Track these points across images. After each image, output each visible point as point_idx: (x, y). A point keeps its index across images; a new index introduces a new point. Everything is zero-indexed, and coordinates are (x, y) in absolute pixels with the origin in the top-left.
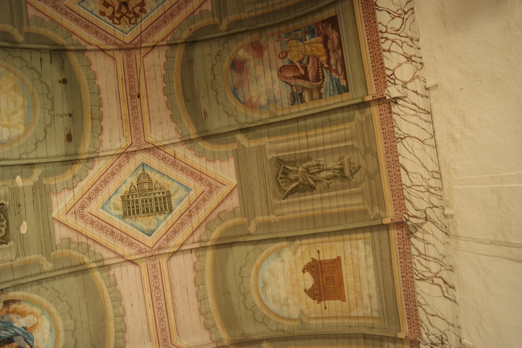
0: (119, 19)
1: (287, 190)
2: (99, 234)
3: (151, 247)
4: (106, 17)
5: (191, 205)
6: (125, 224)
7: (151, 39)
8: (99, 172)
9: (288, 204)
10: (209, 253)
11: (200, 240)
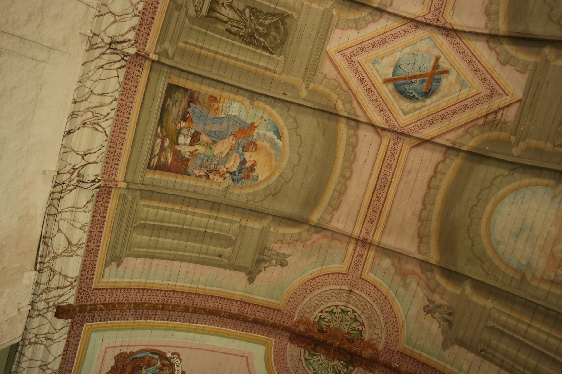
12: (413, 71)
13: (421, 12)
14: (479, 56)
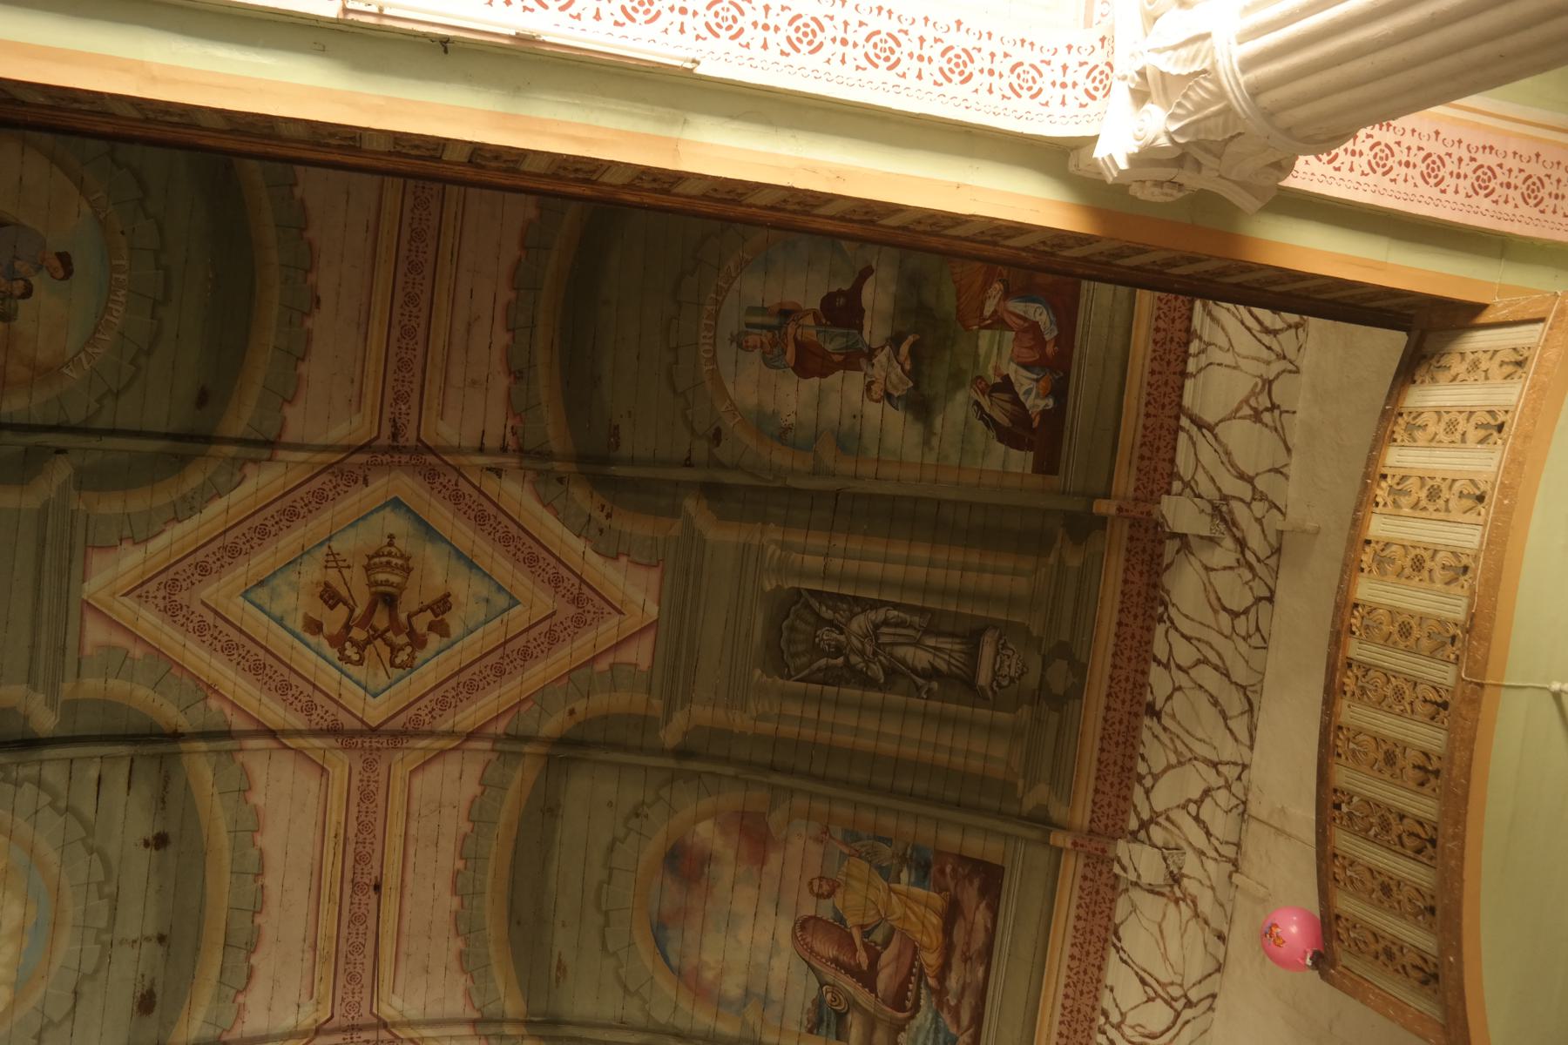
0: (361, 647)
4: (321, 636)
7: (446, 721)
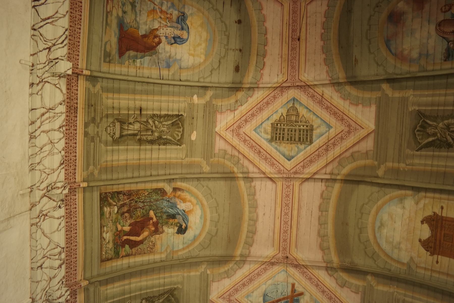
1: (422, 143)
2: (248, 151)
3: (289, 170)
5: (329, 141)
6: (270, 147)
8: (256, 100)
9: (420, 156)
10: (337, 186)
11: (331, 173)
12: (277, 296)
13: (273, 253)
14: (323, 281)
